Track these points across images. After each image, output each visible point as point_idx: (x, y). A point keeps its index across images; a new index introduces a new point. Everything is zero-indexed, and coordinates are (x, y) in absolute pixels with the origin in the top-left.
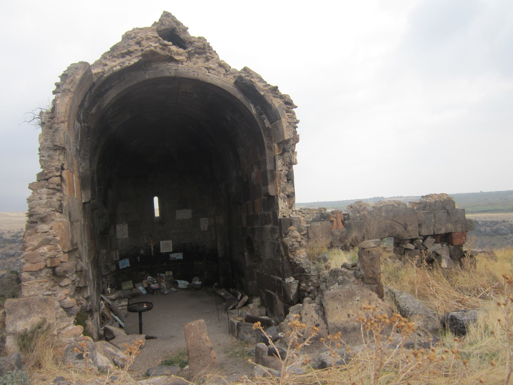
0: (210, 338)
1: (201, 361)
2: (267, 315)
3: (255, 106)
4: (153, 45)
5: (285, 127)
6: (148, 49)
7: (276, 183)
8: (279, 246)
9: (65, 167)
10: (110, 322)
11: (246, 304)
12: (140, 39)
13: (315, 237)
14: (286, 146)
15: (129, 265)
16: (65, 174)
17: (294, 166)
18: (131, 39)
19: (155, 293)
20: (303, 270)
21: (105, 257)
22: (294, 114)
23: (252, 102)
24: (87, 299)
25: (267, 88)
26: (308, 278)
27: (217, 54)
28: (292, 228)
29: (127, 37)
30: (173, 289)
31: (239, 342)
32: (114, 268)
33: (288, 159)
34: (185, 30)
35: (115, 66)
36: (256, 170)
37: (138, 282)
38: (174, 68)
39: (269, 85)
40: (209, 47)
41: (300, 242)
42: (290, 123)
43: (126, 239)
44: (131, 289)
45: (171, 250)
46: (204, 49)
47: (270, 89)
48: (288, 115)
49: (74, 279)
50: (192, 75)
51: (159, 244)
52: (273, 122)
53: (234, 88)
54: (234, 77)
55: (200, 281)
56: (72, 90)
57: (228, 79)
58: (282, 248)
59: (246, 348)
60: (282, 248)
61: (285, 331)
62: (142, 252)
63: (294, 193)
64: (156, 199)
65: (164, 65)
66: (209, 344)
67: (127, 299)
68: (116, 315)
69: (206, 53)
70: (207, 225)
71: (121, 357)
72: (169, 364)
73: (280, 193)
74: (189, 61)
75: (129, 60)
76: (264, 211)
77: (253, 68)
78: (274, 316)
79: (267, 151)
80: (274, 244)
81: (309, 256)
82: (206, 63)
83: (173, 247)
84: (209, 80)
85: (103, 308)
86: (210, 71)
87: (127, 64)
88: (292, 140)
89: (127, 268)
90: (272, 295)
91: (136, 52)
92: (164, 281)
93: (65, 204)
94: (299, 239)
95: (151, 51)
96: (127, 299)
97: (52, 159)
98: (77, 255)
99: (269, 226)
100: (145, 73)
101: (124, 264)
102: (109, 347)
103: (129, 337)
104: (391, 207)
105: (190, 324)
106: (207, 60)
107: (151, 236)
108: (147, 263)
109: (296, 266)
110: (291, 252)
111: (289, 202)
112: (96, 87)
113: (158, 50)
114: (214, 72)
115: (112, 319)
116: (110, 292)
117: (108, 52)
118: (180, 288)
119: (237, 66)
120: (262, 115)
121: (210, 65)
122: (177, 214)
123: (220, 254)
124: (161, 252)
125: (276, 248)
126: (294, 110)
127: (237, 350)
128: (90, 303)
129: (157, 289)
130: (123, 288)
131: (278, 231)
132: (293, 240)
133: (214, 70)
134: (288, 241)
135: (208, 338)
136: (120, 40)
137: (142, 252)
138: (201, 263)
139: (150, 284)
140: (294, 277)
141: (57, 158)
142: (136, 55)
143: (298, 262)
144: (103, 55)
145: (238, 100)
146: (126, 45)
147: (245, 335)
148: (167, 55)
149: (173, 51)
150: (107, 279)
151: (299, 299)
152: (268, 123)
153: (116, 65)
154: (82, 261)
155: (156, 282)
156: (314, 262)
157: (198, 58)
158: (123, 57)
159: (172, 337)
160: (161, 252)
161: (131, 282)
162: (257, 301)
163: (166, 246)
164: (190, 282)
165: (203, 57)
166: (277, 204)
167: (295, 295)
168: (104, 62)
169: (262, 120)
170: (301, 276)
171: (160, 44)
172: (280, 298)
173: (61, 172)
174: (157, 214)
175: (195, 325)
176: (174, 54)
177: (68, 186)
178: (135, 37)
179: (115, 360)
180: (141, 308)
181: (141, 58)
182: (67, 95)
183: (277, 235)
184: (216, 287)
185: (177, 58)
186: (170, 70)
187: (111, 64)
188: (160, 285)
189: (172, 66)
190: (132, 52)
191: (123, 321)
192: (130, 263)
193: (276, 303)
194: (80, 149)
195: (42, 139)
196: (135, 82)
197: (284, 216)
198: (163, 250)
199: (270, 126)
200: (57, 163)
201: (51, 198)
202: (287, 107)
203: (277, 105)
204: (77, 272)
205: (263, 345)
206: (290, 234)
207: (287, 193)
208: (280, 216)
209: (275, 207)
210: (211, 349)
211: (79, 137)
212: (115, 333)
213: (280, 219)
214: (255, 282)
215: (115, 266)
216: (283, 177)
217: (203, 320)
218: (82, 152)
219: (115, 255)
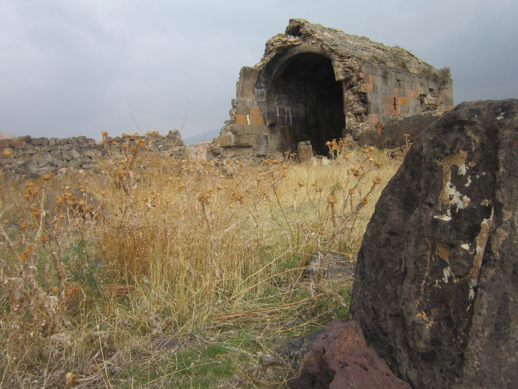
4: (278, 43)
50: (305, 50)
84: (313, 51)
95: (278, 47)
104: (417, 117)
113: (282, 45)
136: (265, 47)
153: (268, 59)
185: (296, 44)
186: (296, 52)
189: (297, 48)
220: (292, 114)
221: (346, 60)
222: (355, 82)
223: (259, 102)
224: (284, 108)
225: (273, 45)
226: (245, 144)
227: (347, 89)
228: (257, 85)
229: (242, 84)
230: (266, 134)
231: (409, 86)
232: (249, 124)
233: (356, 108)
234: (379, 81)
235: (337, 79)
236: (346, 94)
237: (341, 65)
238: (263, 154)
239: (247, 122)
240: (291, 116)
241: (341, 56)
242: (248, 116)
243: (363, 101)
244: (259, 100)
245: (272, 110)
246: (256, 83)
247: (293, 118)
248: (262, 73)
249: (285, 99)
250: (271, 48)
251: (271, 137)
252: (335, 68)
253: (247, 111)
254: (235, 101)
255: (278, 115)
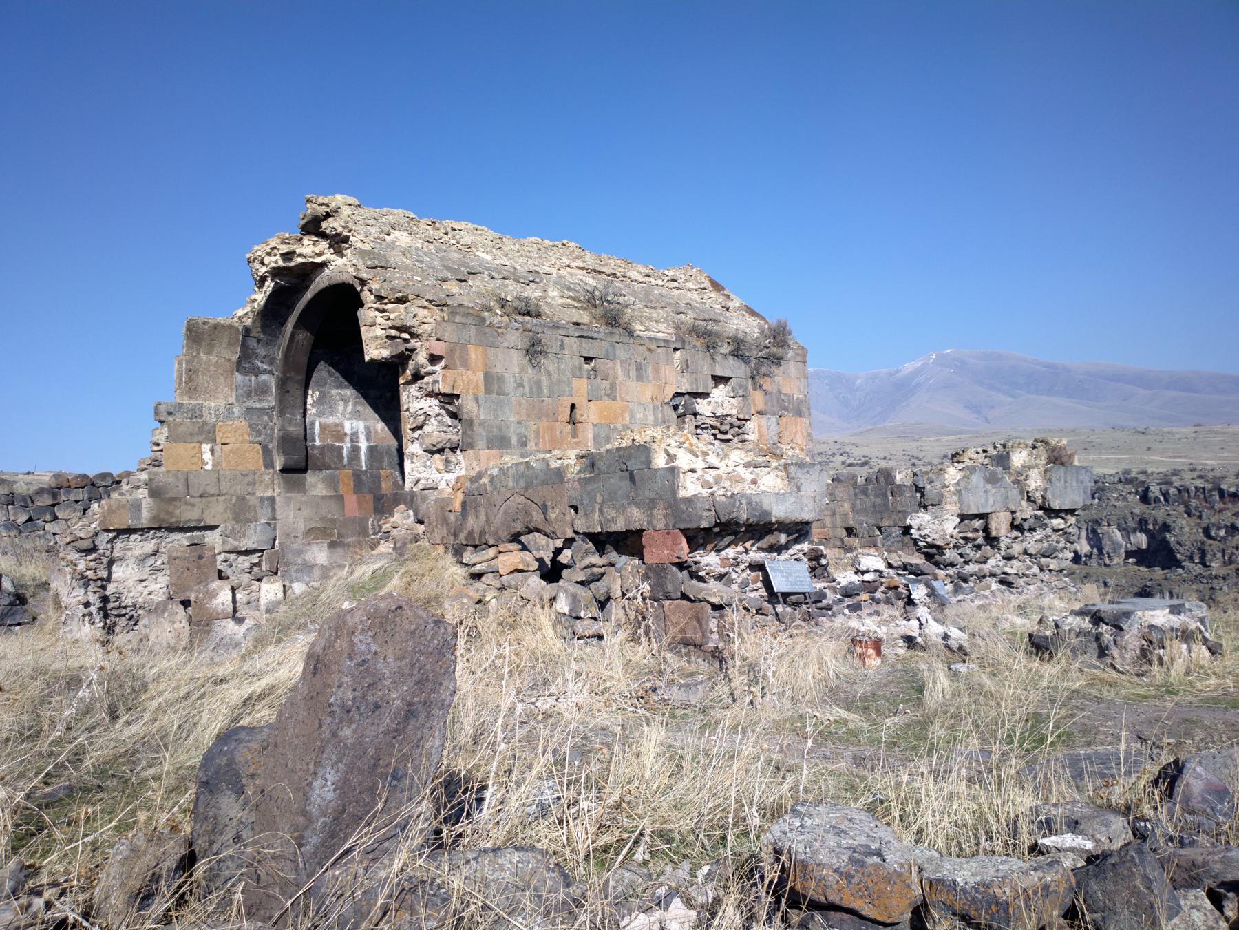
4: (273, 259)
50: (339, 279)
113: (281, 263)
185: (318, 260)
220: (368, 439)
221: (390, 306)
222: (423, 366)
223: (249, 411)
224: (342, 425)
225: (262, 263)
226: (189, 520)
227: (408, 383)
228: (245, 364)
229: (188, 362)
230: (269, 493)
231: (633, 372)
232: (209, 467)
233: (429, 435)
234: (511, 364)
235: (367, 359)
236: (404, 397)
237: (379, 320)
238: (253, 547)
239: (203, 462)
240: (363, 445)
241: (380, 298)
242: (206, 448)
243: (454, 415)
244: (251, 404)
245: (291, 429)
246: (239, 362)
247: (371, 449)
248: (254, 333)
249: (345, 401)
250: (263, 270)
251: (288, 501)
252: (363, 329)
253: (208, 433)
254: (162, 409)
255: (317, 443)
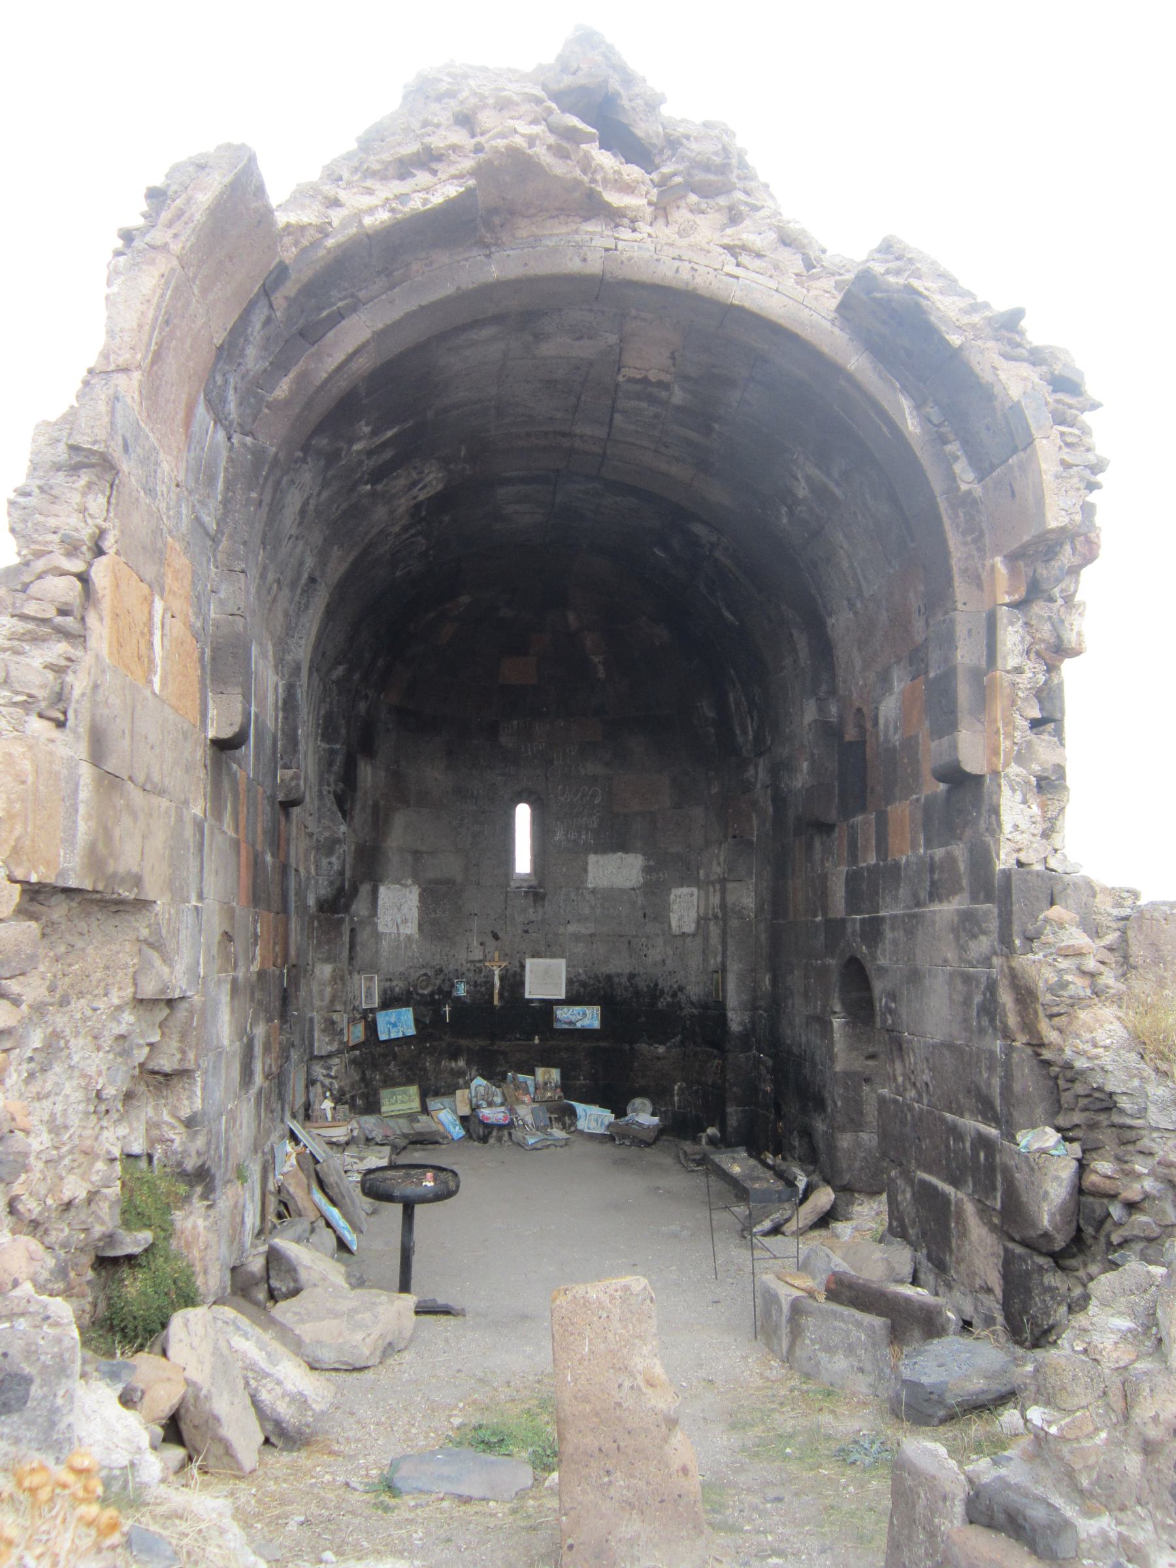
0: (666, 1367)
1: (619, 1479)
2: (915, 1282)
3: (918, 407)
4: (524, 128)
5: (1048, 478)
6: (501, 143)
7: (995, 721)
8: (992, 987)
9: (109, 543)
10: (302, 1226)
11: (824, 1220)
12: (473, 101)
13: (1156, 963)
14: (1042, 571)
15: (411, 1031)
16: (100, 573)
17: (1068, 667)
18: (439, 99)
19: (492, 1141)
20: (1105, 1103)
21: (329, 989)
22: (1086, 431)
23: (905, 389)
24: (190, 1123)
25: (976, 318)
26: (1127, 1138)
27: (772, 196)
28: (1055, 912)
29: (424, 91)
30: (558, 1133)
31: (795, 1382)
32: (358, 1033)
33: (1047, 627)
34: (652, 106)
35: (371, 211)
36: (899, 683)
37: (437, 1094)
38: (599, 242)
39: (986, 306)
40: (743, 165)
41: (1092, 975)
42: (1066, 465)
43: (409, 938)
44: (411, 1117)
45: (563, 997)
46: (723, 169)
47: (989, 321)
48: (1062, 434)
49: (123, 1029)
51: (523, 967)
52: (993, 467)
53: (837, 331)
54: (838, 286)
55: (653, 1115)
56: (176, 247)
57: (813, 293)
58: (1006, 998)
59: (826, 1418)
60: (1006, 998)
61: (1070, 1403)
62: (461, 990)
63: (1060, 770)
64: (523, 814)
65: (563, 230)
66: (662, 1401)
67: (387, 1149)
68: (334, 1202)
69: (727, 189)
70: (693, 915)
71: (289, 1387)
72: (488, 1445)
73: (1006, 765)
74: (661, 222)
75: (427, 190)
76: (928, 844)
77: (919, 240)
78: (949, 1287)
79: (961, 589)
80: (968, 979)
81: (1139, 1042)
82: (729, 231)
83: (570, 982)
85: (286, 1169)
86: (744, 259)
87: (416, 204)
88: (1068, 548)
89: (406, 1040)
90: (945, 1198)
91: (453, 157)
92: (526, 1099)
93: (78, 684)
94: (1091, 964)
95: (514, 153)
96: (387, 1149)
97: (55, 499)
98: (145, 932)
99: (947, 909)
100: (488, 256)
101: (395, 1025)
102: (245, 1335)
103: (353, 1298)
105: (579, 1290)
106: (734, 217)
107: (496, 937)
108: (475, 1030)
109: (1072, 1081)
110: (1051, 1016)
111: (1043, 807)
112: (290, 288)
113: (541, 153)
114: (757, 263)
115: (312, 1215)
116: (329, 1115)
117: (349, 156)
118: (581, 1132)
119: (848, 241)
120: (945, 442)
121: (744, 236)
122: (590, 868)
123: (736, 1021)
124: (527, 996)
125: (978, 999)
126: (1087, 418)
127: (787, 1421)
128: (200, 1142)
129: (501, 1127)
130: (383, 1109)
131: (993, 925)
132: (1063, 964)
133: (759, 256)
134: (1039, 967)
135: (659, 1370)
137: (461, 990)
138: (661, 1049)
139: (479, 1107)
140: (1058, 1129)
141: (76, 498)
142: (453, 170)
143: (1081, 1063)
144: (327, 168)
145: (850, 378)
146: (416, 125)
147: (823, 1357)
148: (578, 183)
149: (602, 167)
150: (329, 1068)
151: (1079, 1230)
152: (970, 476)
153: (373, 208)
154: (167, 960)
155: (498, 1100)
156: (1164, 1066)
157: (697, 210)
158: (402, 177)
159: (524, 1317)
160: (527, 996)
161: (413, 1090)
162: (869, 1214)
163: (545, 980)
164: (620, 1112)
165: (719, 209)
166: (995, 811)
167: (1063, 1209)
168: (329, 190)
169: (947, 463)
170: (1093, 1126)
171: (552, 129)
172: (984, 1212)
173: (90, 565)
174: (523, 863)
175: (605, 1298)
176: (605, 181)
177: (107, 620)
178: (451, 94)
179: (264, 1396)
180: (409, 1189)
181: (472, 182)
182: (152, 262)
183: (983, 944)
184: (712, 1141)
185: (614, 199)
186: (588, 248)
187: (355, 201)
188: (512, 1110)
190: (439, 158)
191: (356, 1228)
192: (417, 1021)
193: (964, 1234)
194: (220, 531)
195: (42, 440)
196: (448, 290)
197: (1020, 864)
198: (534, 990)
199: (978, 489)
200: (74, 520)
201: (16, 652)
202: (1058, 401)
203: (1015, 391)
204: (140, 1003)
205: (934, 1455)
206: (1051, 939)
207: (1035, 767)
208: (1004, 860)
209: (982, 825)
210: (672, 1423)
211: (220, 485)
212: (303, 1275)
213: (1007, 874)
214: (864, 1136)
215: (361, 1027)
216: (1025, 699)
217: (644, 1281)
218: (225, 543)
219: (367, 990)
